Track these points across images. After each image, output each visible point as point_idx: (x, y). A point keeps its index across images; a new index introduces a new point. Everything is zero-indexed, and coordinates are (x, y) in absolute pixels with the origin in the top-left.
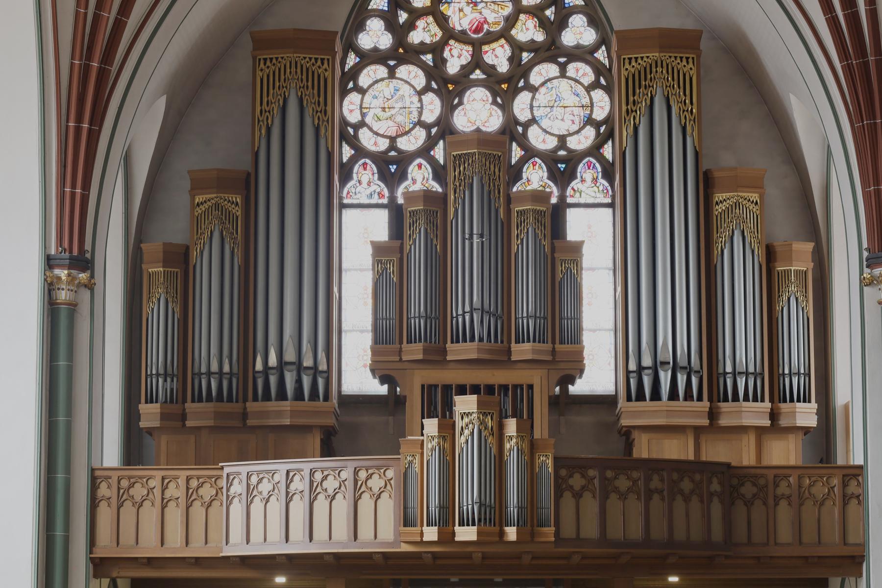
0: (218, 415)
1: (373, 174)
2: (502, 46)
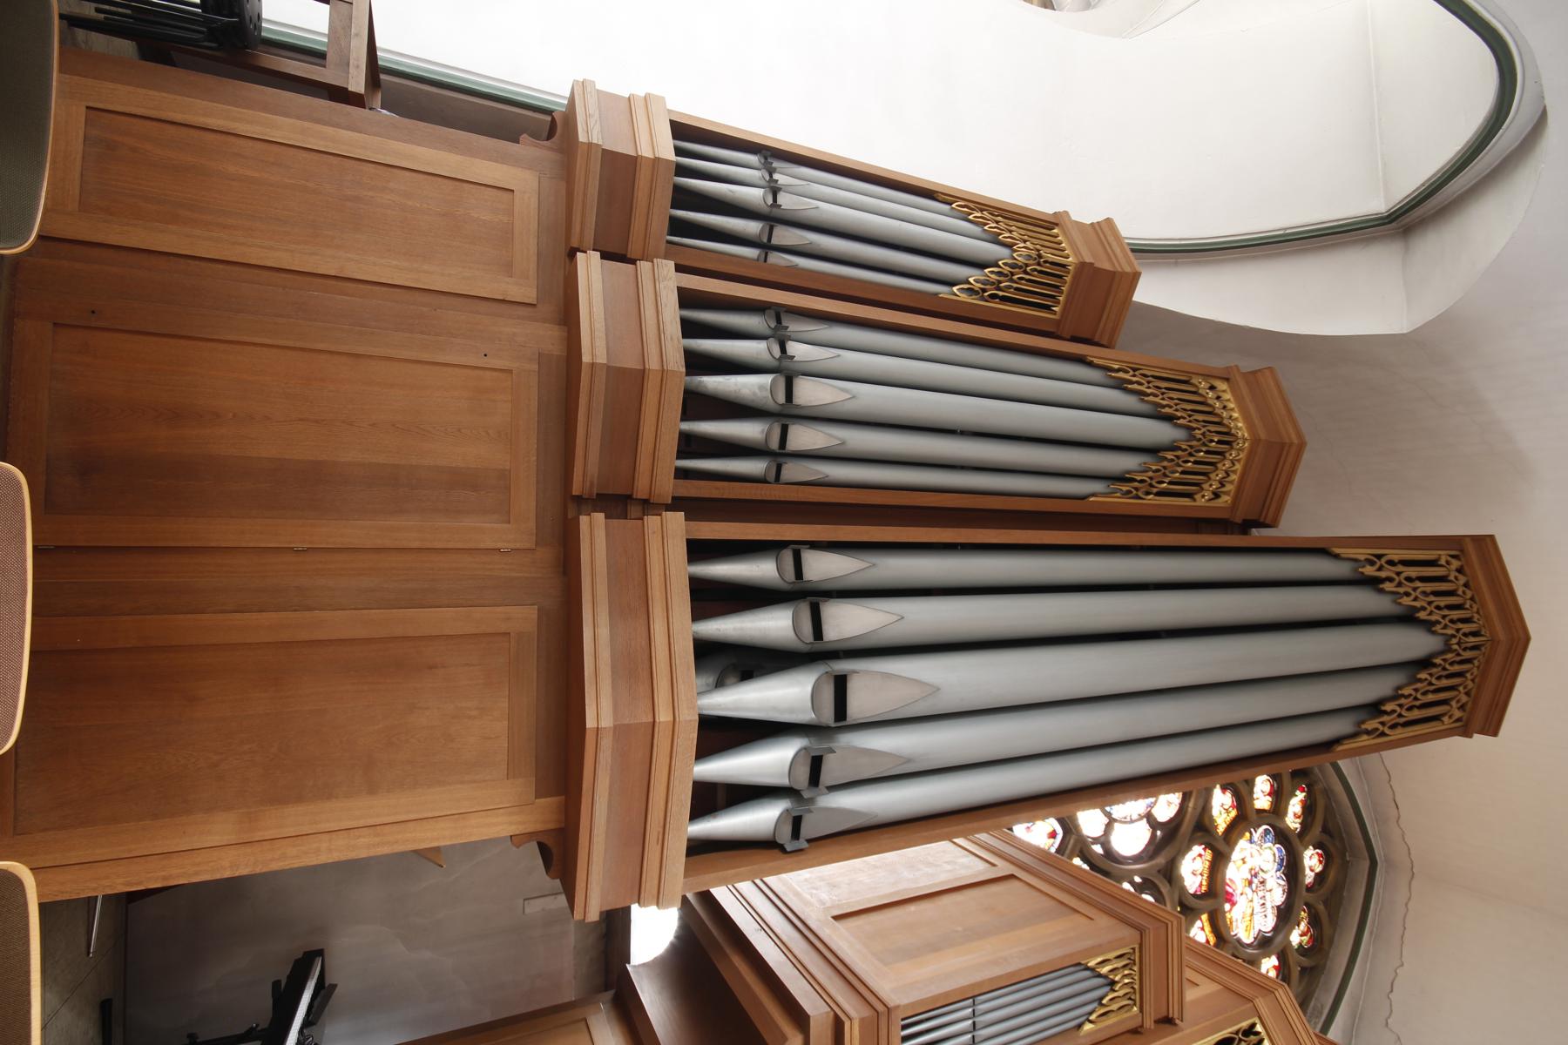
0: (629, 384)
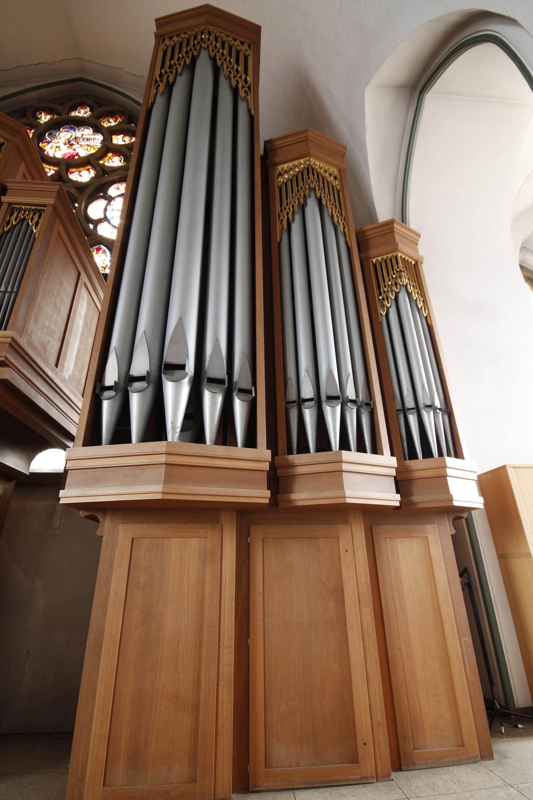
2: (88, 170)
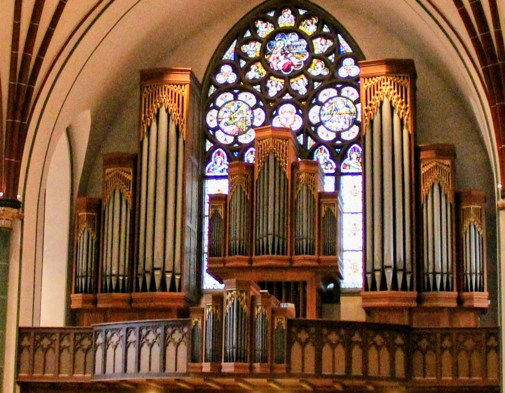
1: (224, 158)
